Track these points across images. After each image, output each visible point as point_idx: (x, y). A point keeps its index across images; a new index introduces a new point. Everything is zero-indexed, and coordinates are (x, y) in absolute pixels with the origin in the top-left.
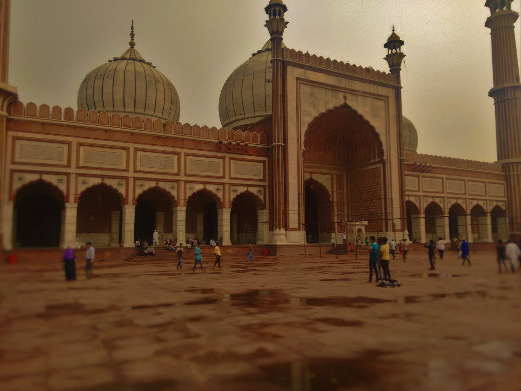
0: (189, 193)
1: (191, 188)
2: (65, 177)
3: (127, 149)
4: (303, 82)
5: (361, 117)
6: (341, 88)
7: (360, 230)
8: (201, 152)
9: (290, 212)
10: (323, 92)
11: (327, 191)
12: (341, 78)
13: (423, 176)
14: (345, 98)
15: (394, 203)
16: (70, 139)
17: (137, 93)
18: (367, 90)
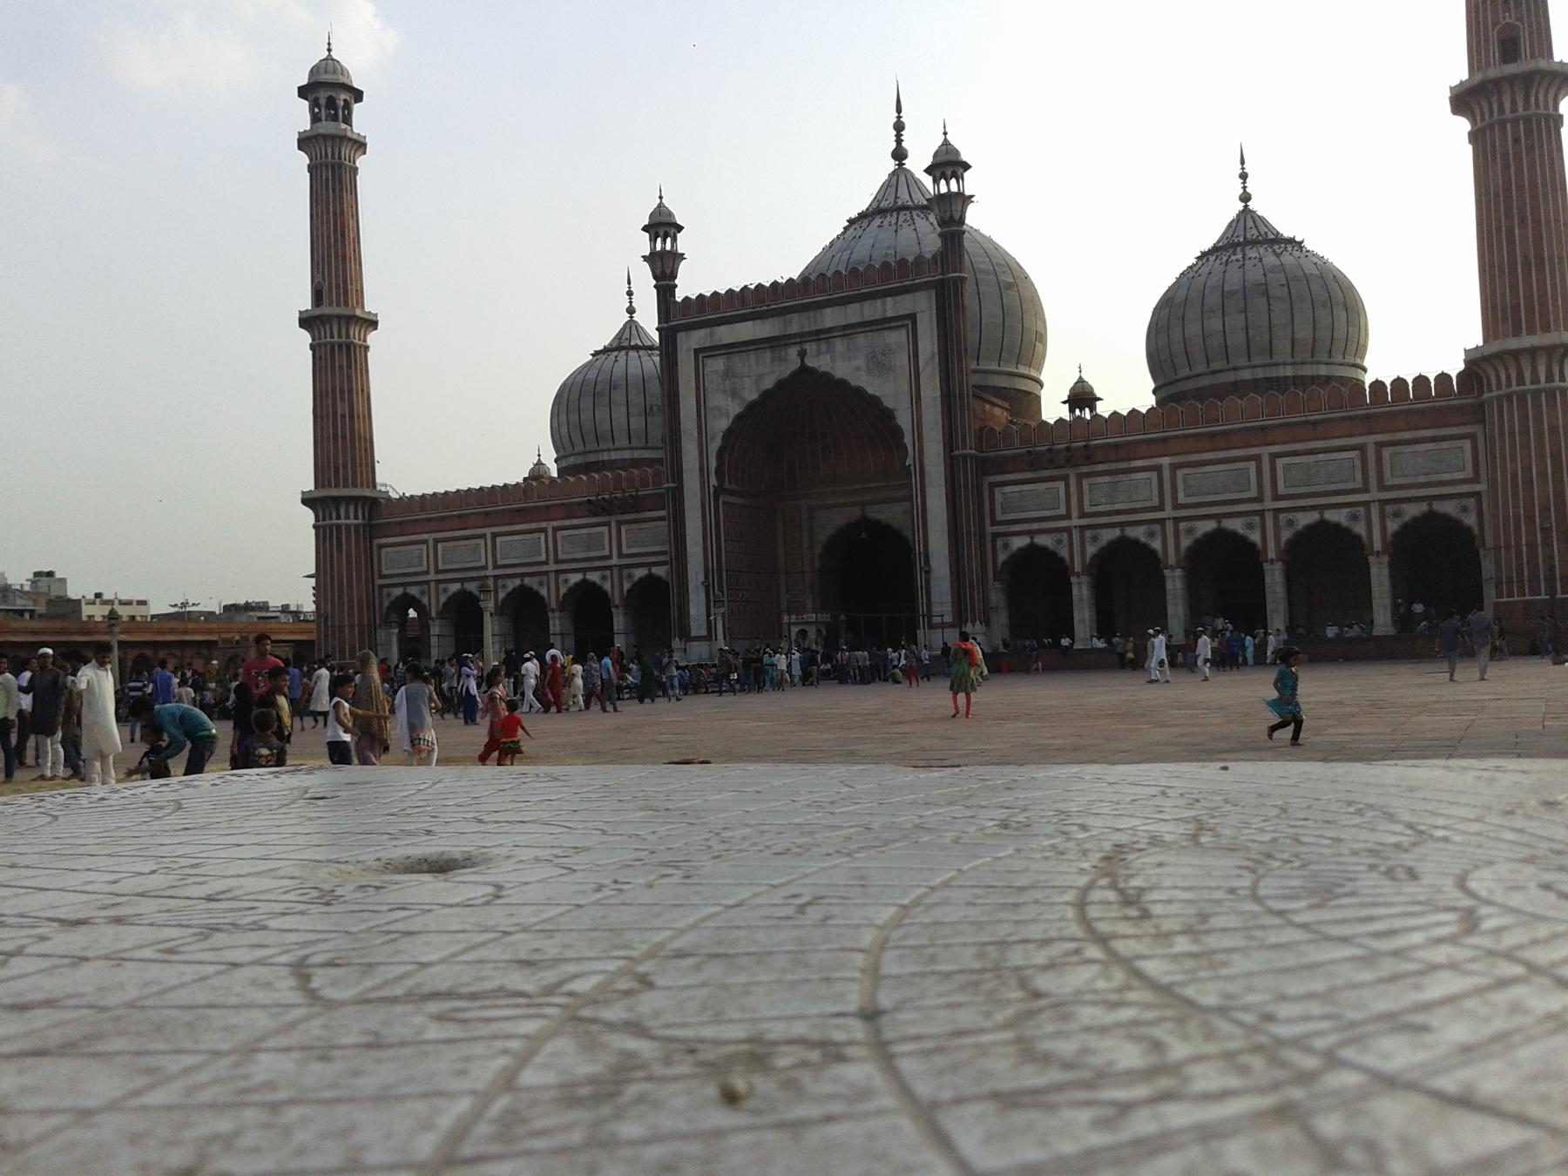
0: (563, 590)
1: (566, 581)
2: (426, 587)
3: (483, 536)
4: (708, 354)
5: (843, 383)
6: (789, 336)
7: (803, 633)
8: (575, 522)
9: (691, 606)
10: (752, 357)
11: (905, 540)
12: (790, 316)
13: (1080, 477)
14: (802, 354)
15: (934, 562)
16: (425, 536)
17: (582, 417)
18: (854, 322)
